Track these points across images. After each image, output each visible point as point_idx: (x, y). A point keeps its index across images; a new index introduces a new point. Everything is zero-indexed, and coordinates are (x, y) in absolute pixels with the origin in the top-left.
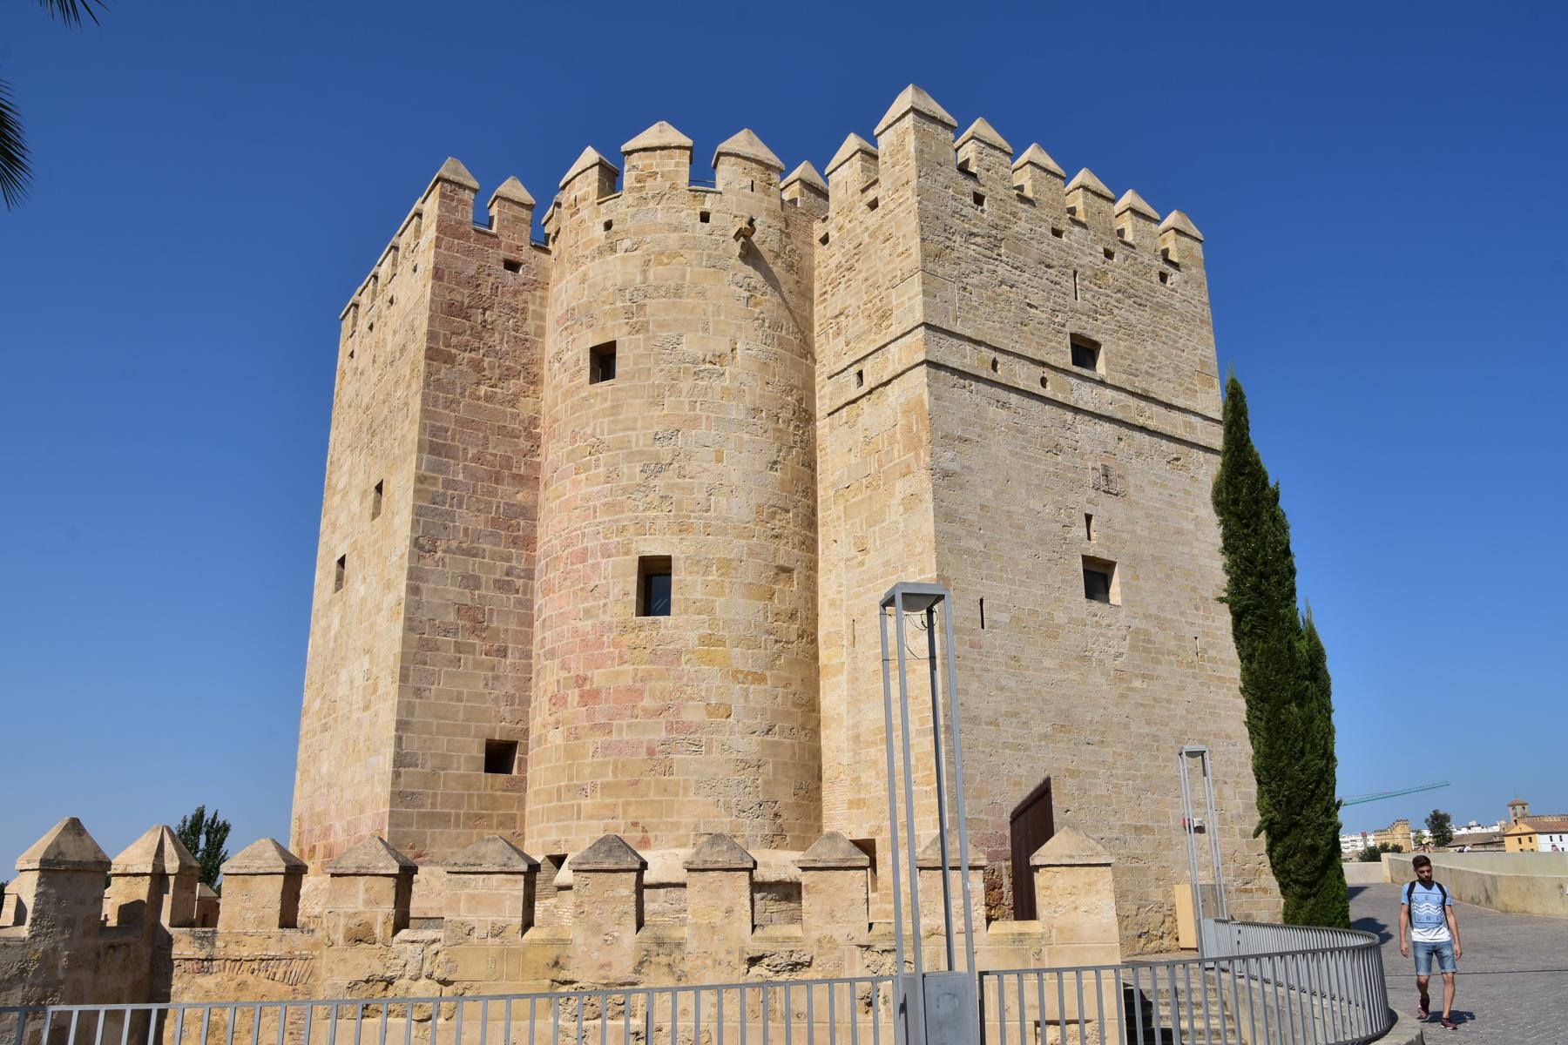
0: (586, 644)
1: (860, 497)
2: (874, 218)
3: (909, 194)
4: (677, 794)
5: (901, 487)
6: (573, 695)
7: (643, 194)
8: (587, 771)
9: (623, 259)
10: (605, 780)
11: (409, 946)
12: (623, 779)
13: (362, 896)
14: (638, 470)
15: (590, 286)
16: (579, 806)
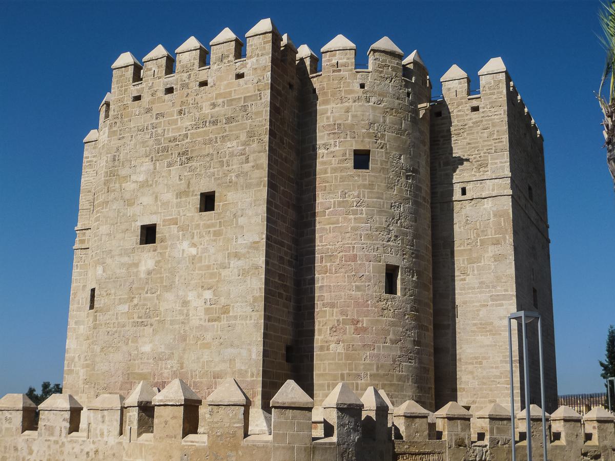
0: (357, 304)
1: (462, 248)
2: (475, 115)
3: (502, 112)
4: (405, 382)
5: (491, 250)
6: (350, 328)
7: (382, 75)
8: (362, 367)
9: (373, 108)
10: (372, 372)
11: (478, 448)
12: (381, 372)
13: (459, 427)
14: (384, 220)
15: (353, 116)
16: (357, 384)
